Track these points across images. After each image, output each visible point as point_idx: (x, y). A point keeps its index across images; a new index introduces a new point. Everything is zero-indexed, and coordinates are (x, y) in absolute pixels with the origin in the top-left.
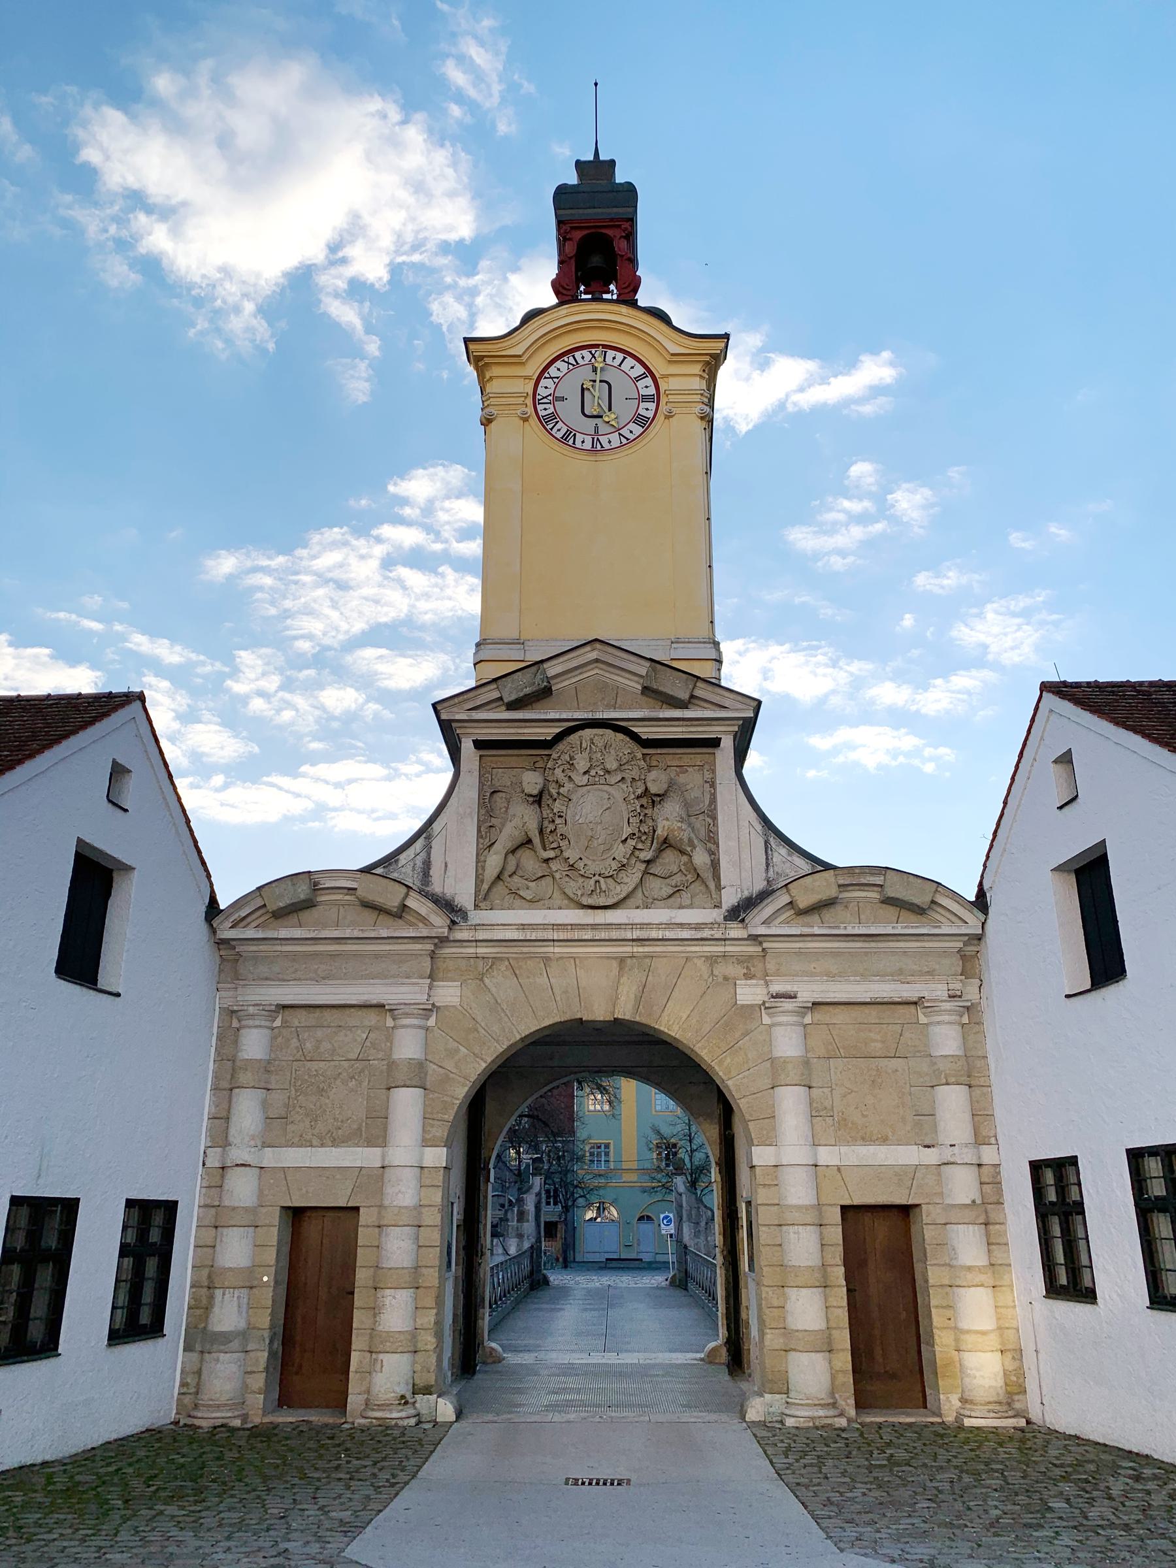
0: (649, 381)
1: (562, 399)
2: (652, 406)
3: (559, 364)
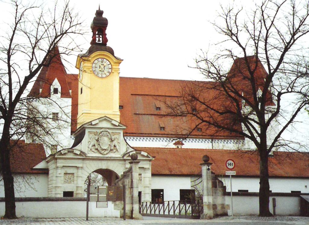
0: (110, 65)
1: (96, 67)
2: (111, 70)
3: (96, 61)
